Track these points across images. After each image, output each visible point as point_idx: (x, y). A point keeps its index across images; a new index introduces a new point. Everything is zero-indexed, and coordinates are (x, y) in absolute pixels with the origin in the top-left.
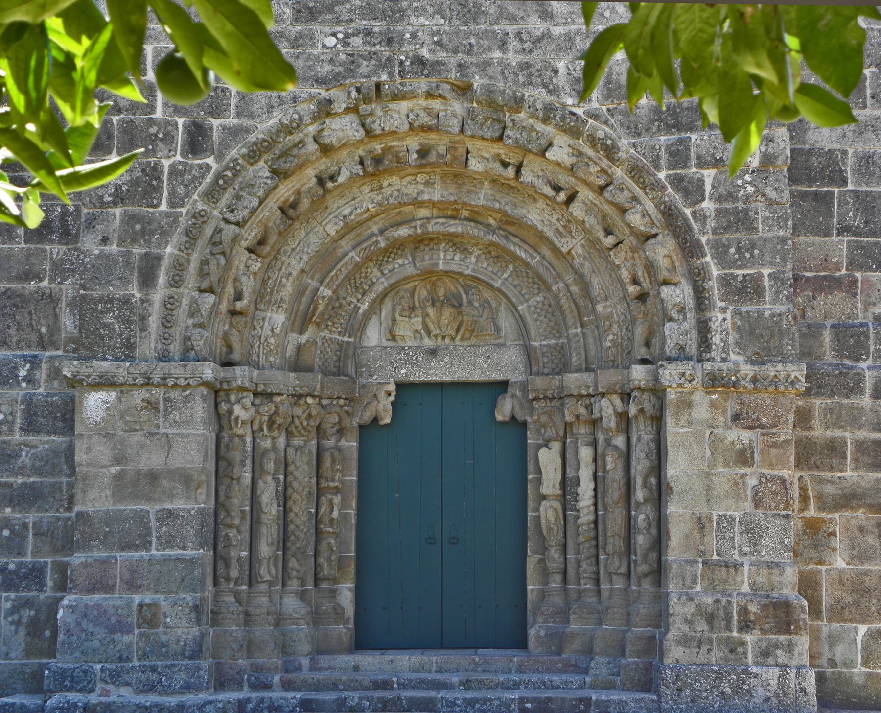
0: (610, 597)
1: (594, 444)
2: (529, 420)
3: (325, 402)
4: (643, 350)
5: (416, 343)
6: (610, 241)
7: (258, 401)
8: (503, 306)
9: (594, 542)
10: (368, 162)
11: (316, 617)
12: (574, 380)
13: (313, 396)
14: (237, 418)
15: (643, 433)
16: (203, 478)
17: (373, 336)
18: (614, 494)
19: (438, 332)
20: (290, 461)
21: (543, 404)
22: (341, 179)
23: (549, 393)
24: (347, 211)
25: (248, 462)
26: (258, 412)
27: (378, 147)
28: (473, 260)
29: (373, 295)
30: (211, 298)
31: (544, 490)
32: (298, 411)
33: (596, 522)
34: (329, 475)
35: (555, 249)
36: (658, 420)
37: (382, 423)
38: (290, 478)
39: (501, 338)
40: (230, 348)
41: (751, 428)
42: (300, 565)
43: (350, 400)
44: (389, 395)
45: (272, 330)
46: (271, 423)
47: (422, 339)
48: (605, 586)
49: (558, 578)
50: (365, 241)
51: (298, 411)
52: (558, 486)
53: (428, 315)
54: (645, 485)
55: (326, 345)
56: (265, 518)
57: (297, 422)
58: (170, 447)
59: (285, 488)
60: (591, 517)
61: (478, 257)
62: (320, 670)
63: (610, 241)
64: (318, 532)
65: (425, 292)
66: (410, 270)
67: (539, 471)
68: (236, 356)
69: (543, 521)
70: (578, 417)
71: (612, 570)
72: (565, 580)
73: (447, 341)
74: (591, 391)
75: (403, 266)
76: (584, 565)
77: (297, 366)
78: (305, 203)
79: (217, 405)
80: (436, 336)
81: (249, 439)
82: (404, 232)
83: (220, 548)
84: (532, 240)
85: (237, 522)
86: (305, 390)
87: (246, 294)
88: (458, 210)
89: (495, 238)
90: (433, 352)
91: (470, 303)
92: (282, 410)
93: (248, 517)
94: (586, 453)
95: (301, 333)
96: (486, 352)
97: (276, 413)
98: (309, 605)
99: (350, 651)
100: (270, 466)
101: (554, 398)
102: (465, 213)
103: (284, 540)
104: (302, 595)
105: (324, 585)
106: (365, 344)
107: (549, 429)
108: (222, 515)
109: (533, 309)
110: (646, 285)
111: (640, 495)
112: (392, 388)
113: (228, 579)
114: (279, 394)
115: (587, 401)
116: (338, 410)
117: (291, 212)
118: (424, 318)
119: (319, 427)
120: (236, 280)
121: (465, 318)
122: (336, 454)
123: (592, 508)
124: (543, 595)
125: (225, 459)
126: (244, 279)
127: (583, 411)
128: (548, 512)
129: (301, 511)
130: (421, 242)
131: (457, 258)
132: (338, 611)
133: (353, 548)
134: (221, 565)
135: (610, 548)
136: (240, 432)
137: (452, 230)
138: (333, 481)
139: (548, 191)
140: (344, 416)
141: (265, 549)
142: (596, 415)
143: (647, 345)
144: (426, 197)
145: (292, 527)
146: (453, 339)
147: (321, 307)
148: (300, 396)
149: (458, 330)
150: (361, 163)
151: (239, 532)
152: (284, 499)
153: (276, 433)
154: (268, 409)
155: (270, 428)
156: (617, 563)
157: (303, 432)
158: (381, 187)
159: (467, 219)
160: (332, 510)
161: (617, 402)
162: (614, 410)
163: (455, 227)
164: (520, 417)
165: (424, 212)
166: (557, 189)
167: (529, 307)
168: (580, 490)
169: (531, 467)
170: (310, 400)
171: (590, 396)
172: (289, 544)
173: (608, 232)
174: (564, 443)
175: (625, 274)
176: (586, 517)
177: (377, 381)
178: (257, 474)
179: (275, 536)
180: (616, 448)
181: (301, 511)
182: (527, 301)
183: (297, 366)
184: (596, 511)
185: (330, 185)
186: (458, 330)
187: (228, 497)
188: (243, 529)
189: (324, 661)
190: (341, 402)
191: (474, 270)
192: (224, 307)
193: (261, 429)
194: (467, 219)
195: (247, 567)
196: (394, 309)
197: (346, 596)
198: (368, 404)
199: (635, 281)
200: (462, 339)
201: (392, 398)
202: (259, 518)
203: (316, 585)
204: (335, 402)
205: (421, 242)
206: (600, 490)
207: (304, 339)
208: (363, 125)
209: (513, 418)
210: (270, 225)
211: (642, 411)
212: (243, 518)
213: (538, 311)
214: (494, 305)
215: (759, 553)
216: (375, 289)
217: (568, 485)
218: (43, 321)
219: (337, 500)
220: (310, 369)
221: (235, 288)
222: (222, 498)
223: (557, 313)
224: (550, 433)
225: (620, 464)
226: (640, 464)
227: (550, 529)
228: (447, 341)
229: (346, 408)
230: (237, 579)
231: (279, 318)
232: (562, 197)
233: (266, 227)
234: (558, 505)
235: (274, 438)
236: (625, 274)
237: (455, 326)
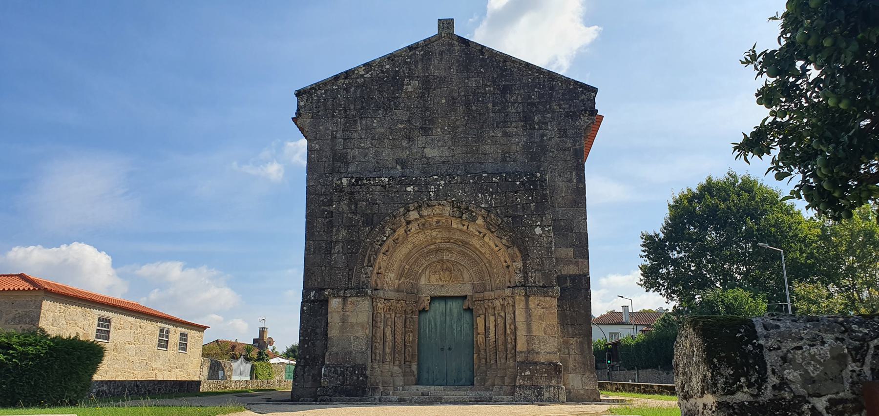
0: (500, 366)
1: (494, 315)
2: (474, 308)
3: (407, 302)
4: (509, 283)
5: (437, 283)
6: (497, 249)
7: (386, 302)
8: (465, 271)
9: (495, 348)
10: (420, 225)
11: (404, 374)
12: (487, 294)
13: (403, 300)
14: (379, 307)
15: (509, 310)
16: (368, 326)
17: (423, 281)
18: (501, 331)
22: (412, 231)
24: (414, 241)
25: (383, 322)
26: (385, 305)
27: (424, 221)
28: (455, 256)
29: (423, 268)
30: (371, 268)
31: (479, 332)
32: (398, 305)
33: (495, 341)
35: (480, 252)
36: (514, 306)
37: (426, 309)
38: (396, 327)
40: (377, 285)
41: (543, 308)
42: (399, 356)
43: (416, 302)
45: (390, 279)
46: (390, 309)
47: (439, 282)
48: (498, 362)
49: (484, 360)
50: (419, 250)
51: (398, 305)
52: (483, 330)
53: (441, 274)
54: (510, 328)
56: (388, 340)
57: (398, 309)
58: (358, 316)
59: (394, 331)
60: (494, 340)
62: (405, 390)
63: (497, 249)
64: (405, 346)
65: (439, 267)
66: (435, 259)
67: (477, 325)
68: (379, 287)
69: (479, 341)
70: (489, 306)
71: (500, 357)
72: (486, 361)
74: (493, 298)
75: (433, 258)
76: (492, 356)
77: (398, 290)
78: (401, 238)
79: (372, 302)
81: (383, 315)
82: (432, 247)
83: (373, 350)
84: (473, 249)
85: (379, 341)
86: (401, 298)
87: (382, 267)
88: (450, 240)
89: (461, 249)
90: (442, 286)
91: (454, 270)
92: (393, 304)
93: (382, 340)
94: (492, 318)
95: (400, 280)
97: (391, 306)
98: (402, 370)
99: (416, 385)
100: (389, 323)
102: (452, 241)
103: (394, 347)
104: (400, 366)
105: (407, 363)
108: (374, 338)
110: (509, 263)
111: (508, 331)
112: (429, 298)
113: (376, 360)
114: (393, 299)
115: (492, 301)
117: (396, 241)
118: (439, 276)
119: (405, 311)
120: (379, 263)
122: (411, 319)
123: (494, 337)
124: (479, 366)
125: (375, 321)
126: (382, 263)
127: (490, 304)
128: (480, 338)
129: (399, 337)
130: (438, 250)
131: (450, 255)
132: (412, 372)
133: (417, 351)
134: (373, 355)
135: (500, 350)
136: (380, 312)
137: (448, 246)
138: (410, 329)
139: (478, 234)
140: (413, 307)
141: (388, 351)
142: (494, 306)
143: (510, 282)
144: (439, 236)
145: (396, 344)
146: (449, 282)
147: (406, 271)
148: (399, 300)
149: (450, 279)
150: (418, 225)
151: (379, 345)
152: (394, 334)
153: (391, 312)
154: (389, 304)
155: (389, 311)
156: (502, 354)
159: (452, 243)
160: (410, 339)
161: (501, 301)
162: (500, 304)
163: (448, 245)
164: (471, 308)
165: (438, 241)
166: (480, 233)
167: (473, 271)
168: (490, 331)
170: (402, 301)
171: (492, 299)
172: (396, 349)
173: (497, 246)
174: (485, 315)
175: (502, 259)
176: (492, 340)
178: (385, 325)
179: (391, 346)
180: (502, 316)
181: (399, 337)
182: (472, 269)
183: (398, 290)
184: (496, 338)
185: (408, 233)
186: (450, 279)
187: (376, 333)
188: (380, 344)
189: (406, 387)
190: (413, 302)
192: (375, 272)
193: (387, 311)
194: (452, 243)
195: (382, 356)
196: (430, 272)
197: (414, 367)
198: (422, 303)
199: (505, 262)
200: (451, 282)
201: (429, 301)
202: (386, 340)
203: (404, 363)
205: (438, 250)
206: (497, 330)
207: (401, 281)
208: (419, 214)
209: (469, 308)
210: (390, 245)
211: (508, 303)
212: (381, 340)
214: (462, 270)
215: (546, 349)
217: (486, 329)
218: (319, 278)
219: (411, 335)
220: (403, 292)
221: (379, 265)
222: (374, 333)
223: (482, 273)
224: (481, 312)
225: (503, 321)
226: (508, 321)
227: (481, 344)
230: (379, 360)
231: (393, 275)
232: (481, 235)
233: (388, 246)
234: (483, 336)
235: (390, 314)
236: (502, 259)
237: (450, 277)
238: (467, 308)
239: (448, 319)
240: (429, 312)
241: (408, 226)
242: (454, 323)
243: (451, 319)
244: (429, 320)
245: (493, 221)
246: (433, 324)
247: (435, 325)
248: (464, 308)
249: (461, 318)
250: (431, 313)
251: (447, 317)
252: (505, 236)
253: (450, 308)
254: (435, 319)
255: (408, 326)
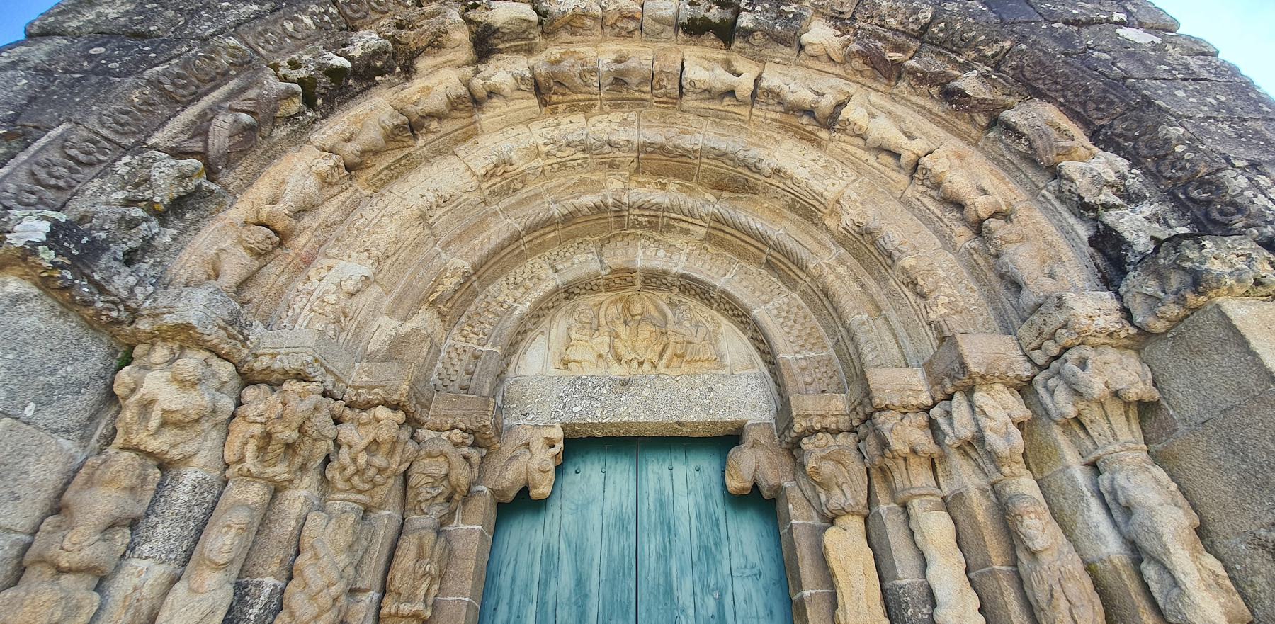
13: (395, 407)
19: (633, 356)
20: (306, 542)
21: (823, 439)
23: (830, 422)
28: (683, 258)
34: (404, 589)
37: (535, 493)
39: (725, 366)
44: (552, 446)
53: (618, 336)
55: (453, 355)
61: (689, 255)
73: (647, 366)
80: (629, 362)
90: (625, 383)
96: (706, 383)
101: (839, 431)
106: (521, 373)
107: (836, 490)
109: (775, 312)
112: (557, 433)
116: (447, 447)
121: (673, 338)
146: (654, 366)
149: (661, 356)
157: (356, 480)
158: (558, 124)
169: (807, 570)
170: (382, 412)
177: (534, 423)
186: (661, 356)
191: (685, 268)
204: (444, 435)
213: (784, 314)
216: (543, 286)
228: (647, 366)
229: (465, 450)
238: (749, 485)
239: (651, 547)
240: (553, 510)
241: (481, 67)
242: (682, 571)
243: (665, 554)
244: (550, 557)
245: (893, 22)
246: (566, 578)
247: (580, 582)
248: (734, 484)
249: (718, 544)
250: (561, 517)
251: (644, 537)
252: (966, 67)
253: (662, 491)
254: (579, 551)
255: (399, 579)
